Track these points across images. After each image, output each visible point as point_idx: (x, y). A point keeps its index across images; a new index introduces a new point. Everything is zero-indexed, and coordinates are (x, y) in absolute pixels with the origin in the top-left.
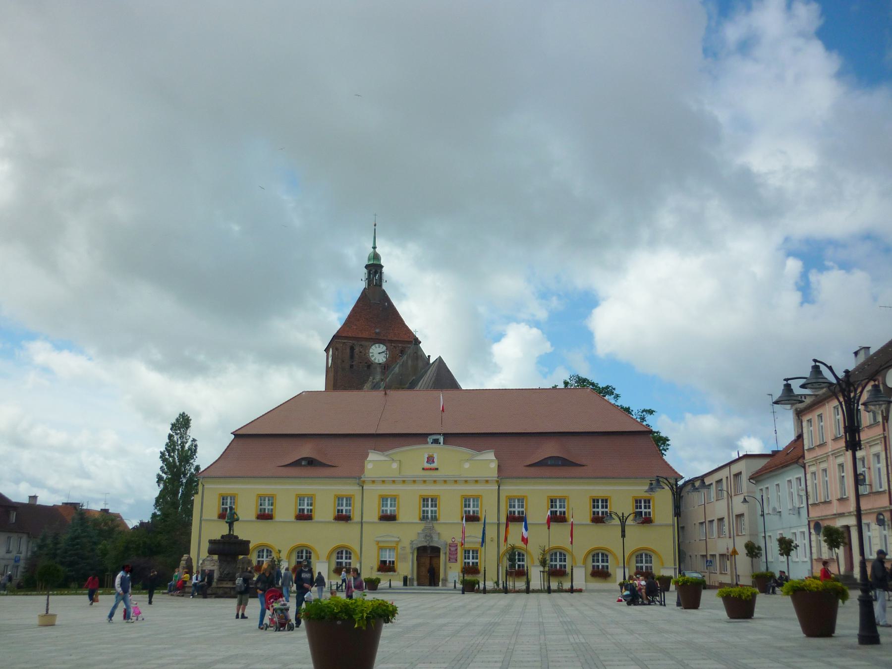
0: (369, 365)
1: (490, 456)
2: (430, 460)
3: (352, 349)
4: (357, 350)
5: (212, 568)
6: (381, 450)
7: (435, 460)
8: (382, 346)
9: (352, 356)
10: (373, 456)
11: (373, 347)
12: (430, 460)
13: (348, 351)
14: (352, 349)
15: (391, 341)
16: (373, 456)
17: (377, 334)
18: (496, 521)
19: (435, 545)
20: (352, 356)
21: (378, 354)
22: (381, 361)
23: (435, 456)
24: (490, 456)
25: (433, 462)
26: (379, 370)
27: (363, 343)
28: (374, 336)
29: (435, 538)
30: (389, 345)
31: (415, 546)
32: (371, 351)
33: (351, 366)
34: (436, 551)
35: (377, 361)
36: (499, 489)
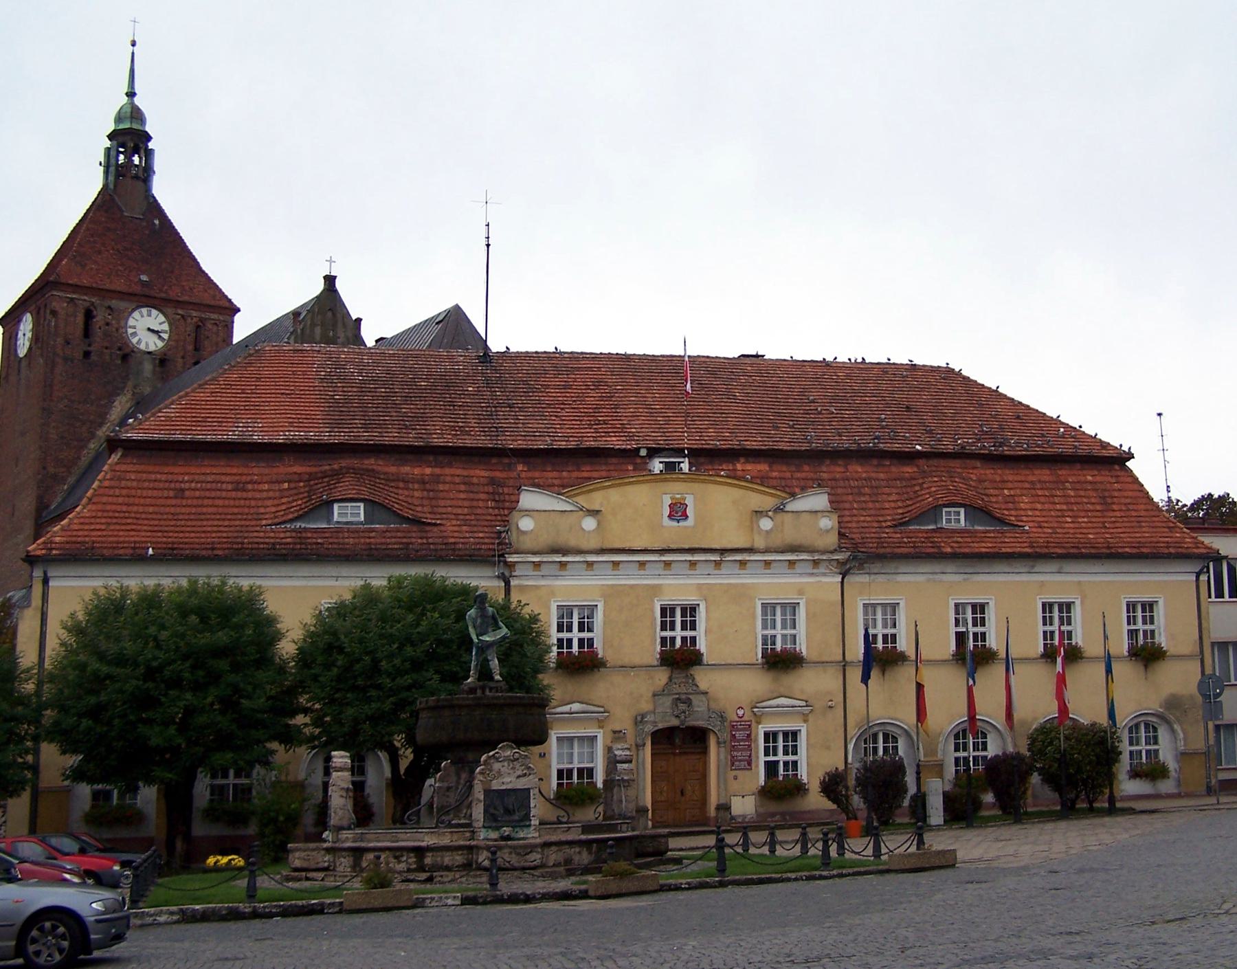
0: (127, 354)
1: (818, 501)
2: (678, 511)
3: (89, 315)
4: (100, 316)
5: (521, 784)
6: (558, 488)
7: (689, 512)
8: (154, 312)
9: (87, 333)
10: (530, 499)
11: (136, 314)
12: (678, 511)
13: (80, 319)
14: (89, 315)
15: (178, 304)
16: (530, 499)
17: (144, 284)
18: (841, 658)
19: (700, 723)
20: (87, 333)
21: (147, 329)
22: (152, 348)
23: (689, 501)
24: (818, 501)
25: (685, 516)
26: (148, 367)
27: (114, 303)
28: (137, 289)
29: (699, 705)
30: (169, 311)
31: (649, 728)
32: (131, 322)
33: (87, 354)
34: (696, 738)
35: (142, 347)
36: (842, 582)
